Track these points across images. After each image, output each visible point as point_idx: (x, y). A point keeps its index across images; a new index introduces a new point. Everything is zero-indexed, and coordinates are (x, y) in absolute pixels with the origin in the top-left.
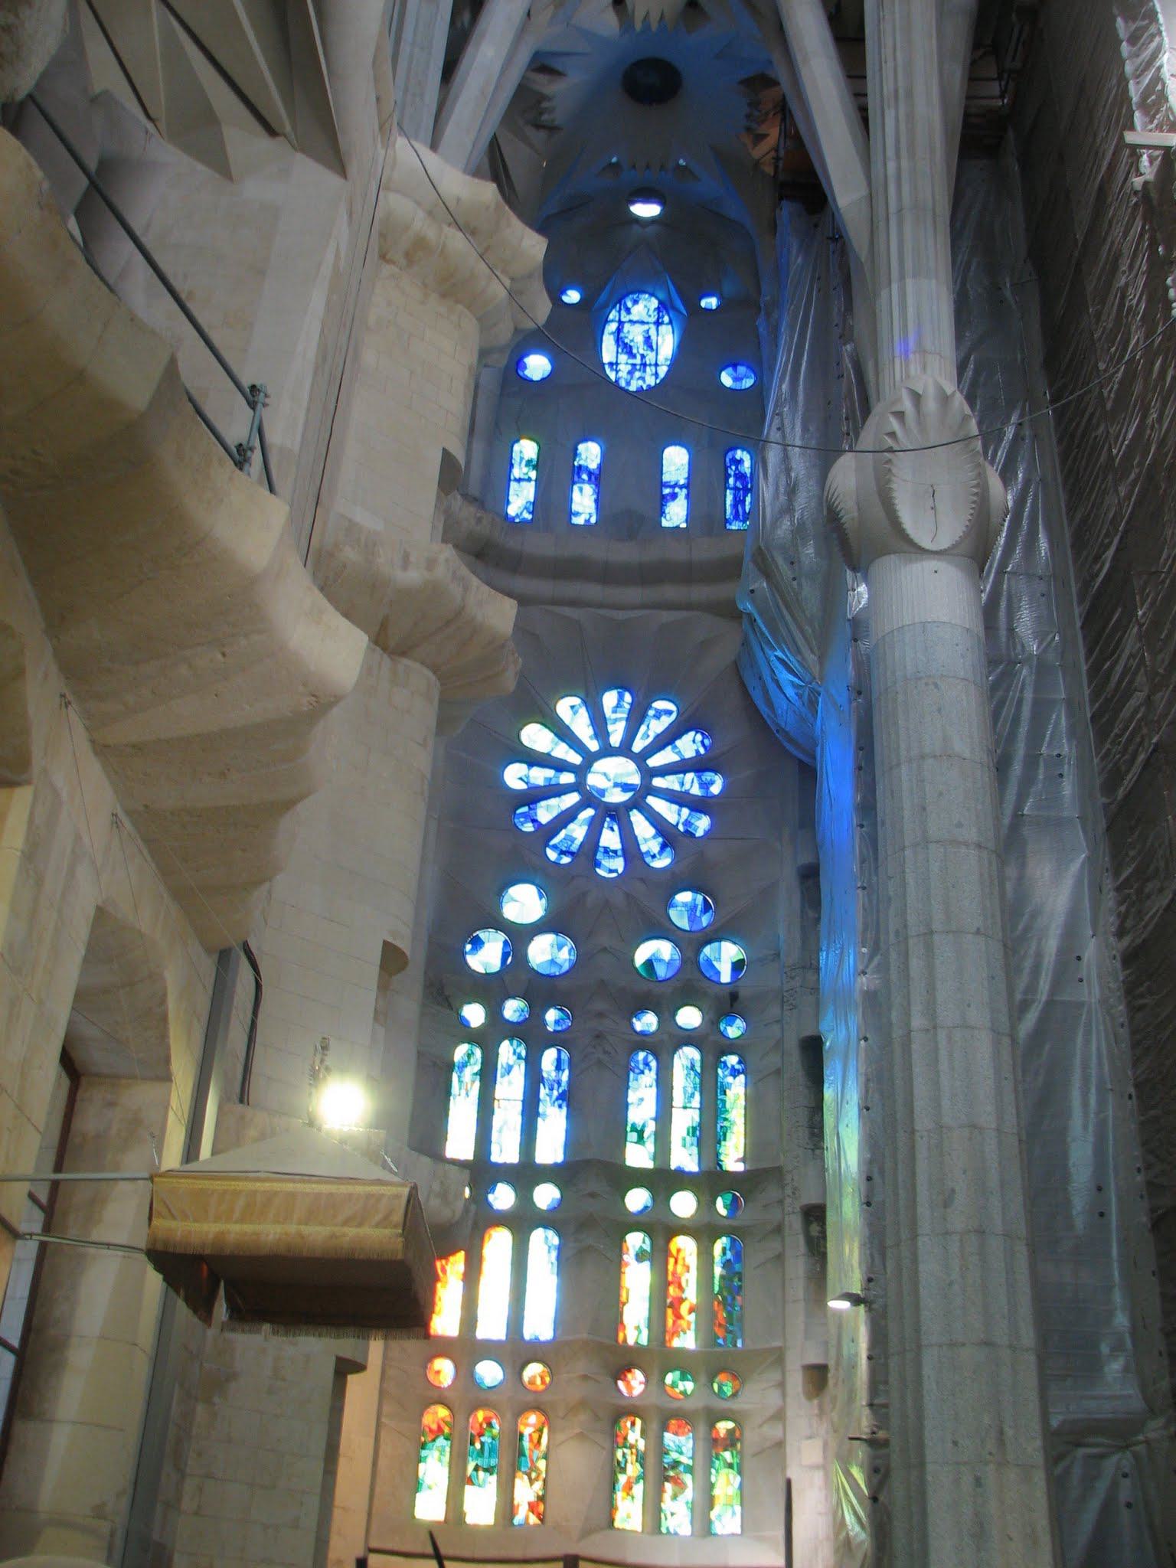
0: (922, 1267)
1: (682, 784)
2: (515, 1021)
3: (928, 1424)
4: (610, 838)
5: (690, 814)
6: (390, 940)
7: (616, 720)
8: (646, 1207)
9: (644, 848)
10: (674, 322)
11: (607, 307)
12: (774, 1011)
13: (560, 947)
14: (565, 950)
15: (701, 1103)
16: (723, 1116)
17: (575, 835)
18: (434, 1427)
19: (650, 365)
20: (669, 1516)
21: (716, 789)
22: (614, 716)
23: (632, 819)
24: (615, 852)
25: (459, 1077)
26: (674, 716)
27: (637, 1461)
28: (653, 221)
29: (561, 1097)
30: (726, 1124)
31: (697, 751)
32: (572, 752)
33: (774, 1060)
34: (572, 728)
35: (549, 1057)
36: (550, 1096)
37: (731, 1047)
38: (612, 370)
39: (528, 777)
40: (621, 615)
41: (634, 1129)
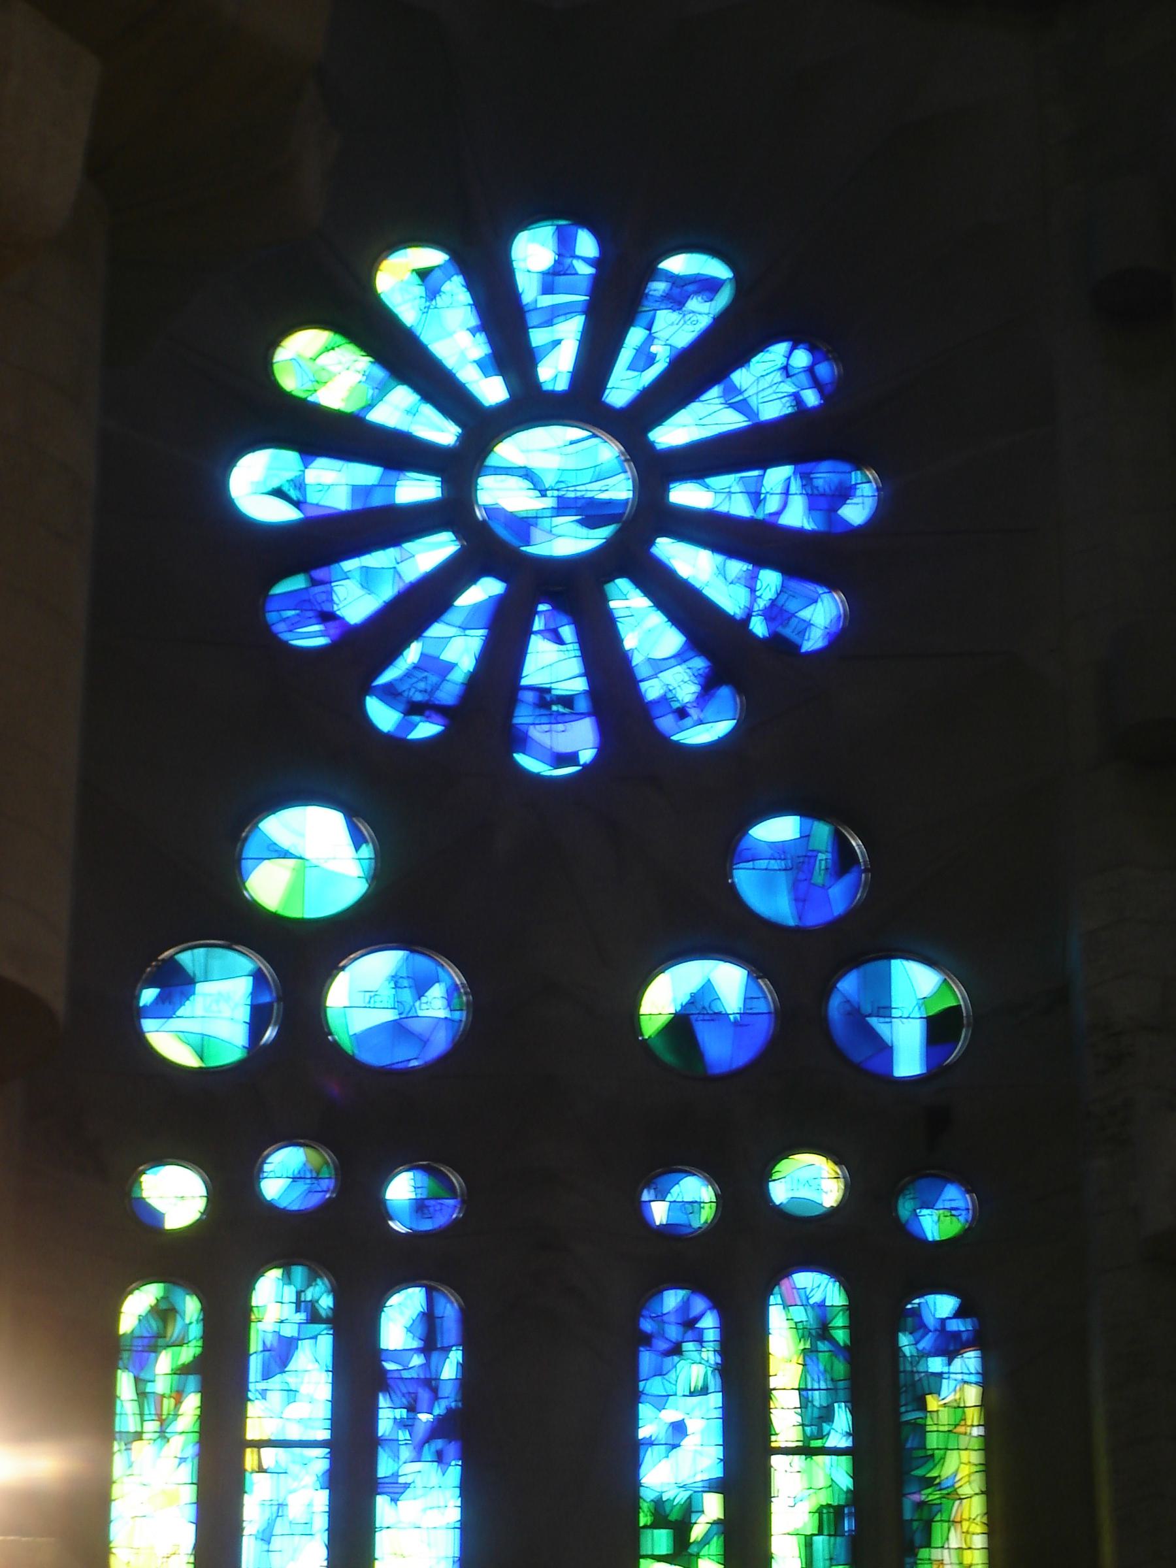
1: (756, 498)
2: (295, 1207)
5: (783, 589)
7: (552, 316)
9: (652, 690)
13: (421, 988)
14: (437, 992)
16: (919, 1472)
17: (447, 656)
21: (856, 512)
22: (547, 301)
24: (567, 701)
25: (137, 1380)
26: (724, 298)
29: (439, 1429)
30: (930, 1495)
31: (797, 398)
32: (428, 410)
34: (426, 337)
39: (300, 485)
41: (660, 1519)
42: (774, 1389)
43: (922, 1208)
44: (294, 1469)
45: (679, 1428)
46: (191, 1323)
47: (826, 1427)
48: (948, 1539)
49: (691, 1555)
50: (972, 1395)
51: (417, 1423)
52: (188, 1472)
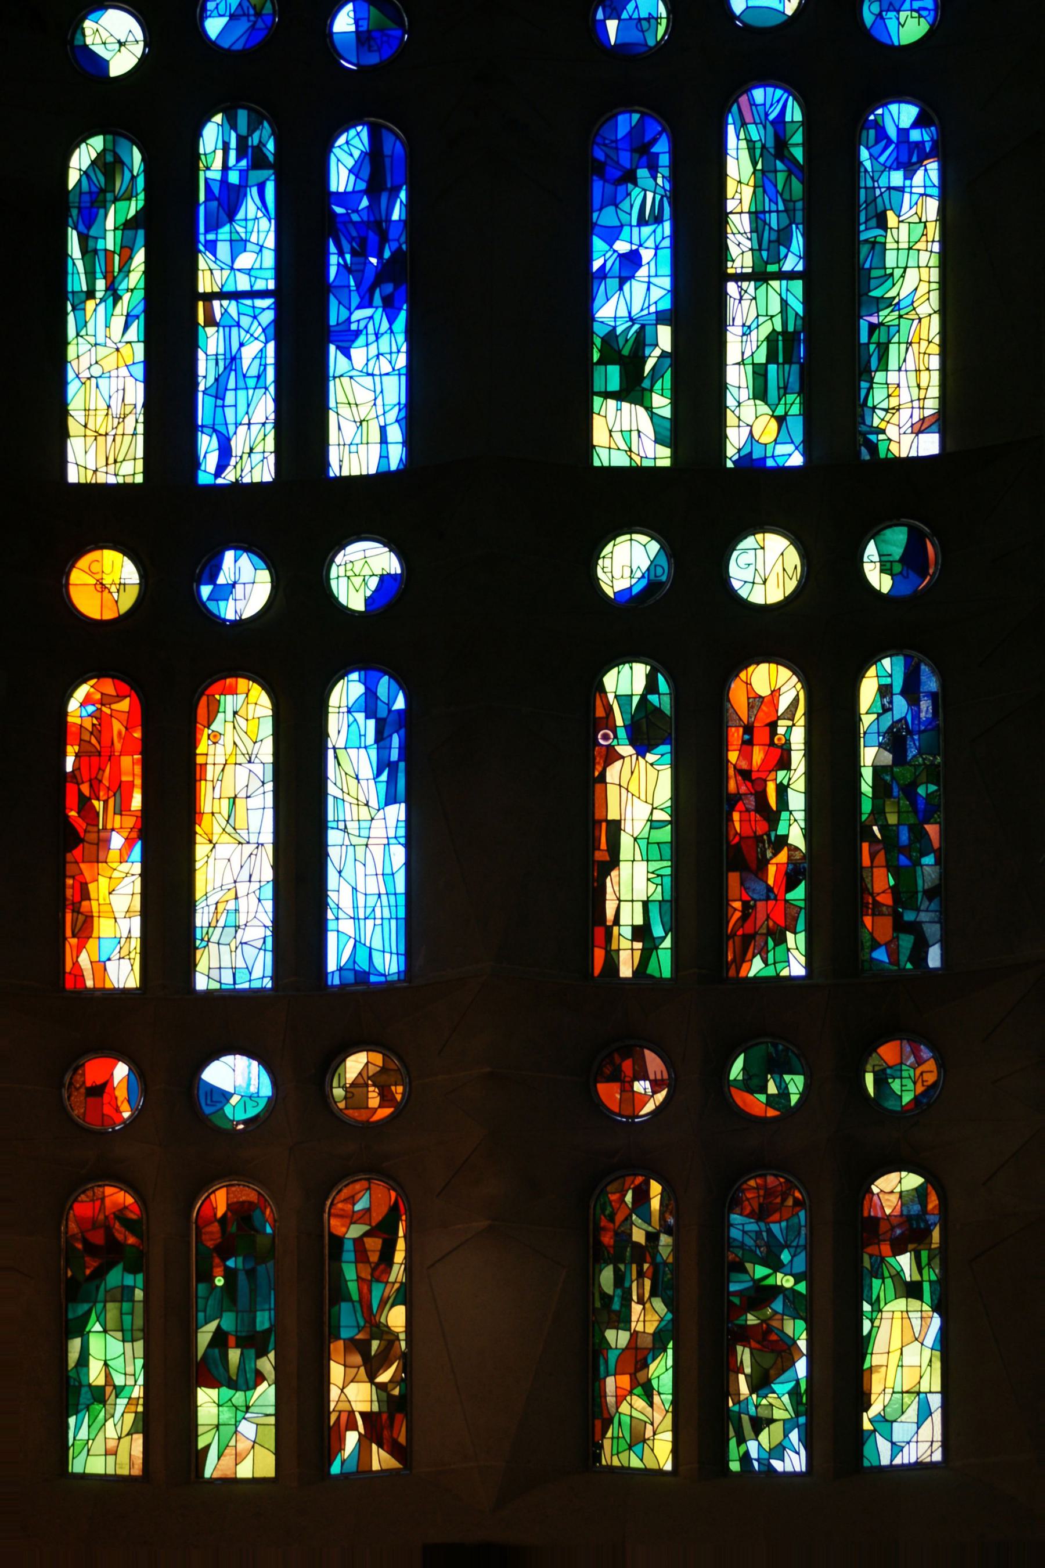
15: (808, 256)
30: (886, 316)
41: (611, 352)
42: (731, 213)
43: (888, 10)
44: (245, 321)
45: (631, 261)
46: (138, 175)
47: (783, 251)
48: (905, 360)
49: (644, 389)
50: (932, 207)
51: (368, 267)
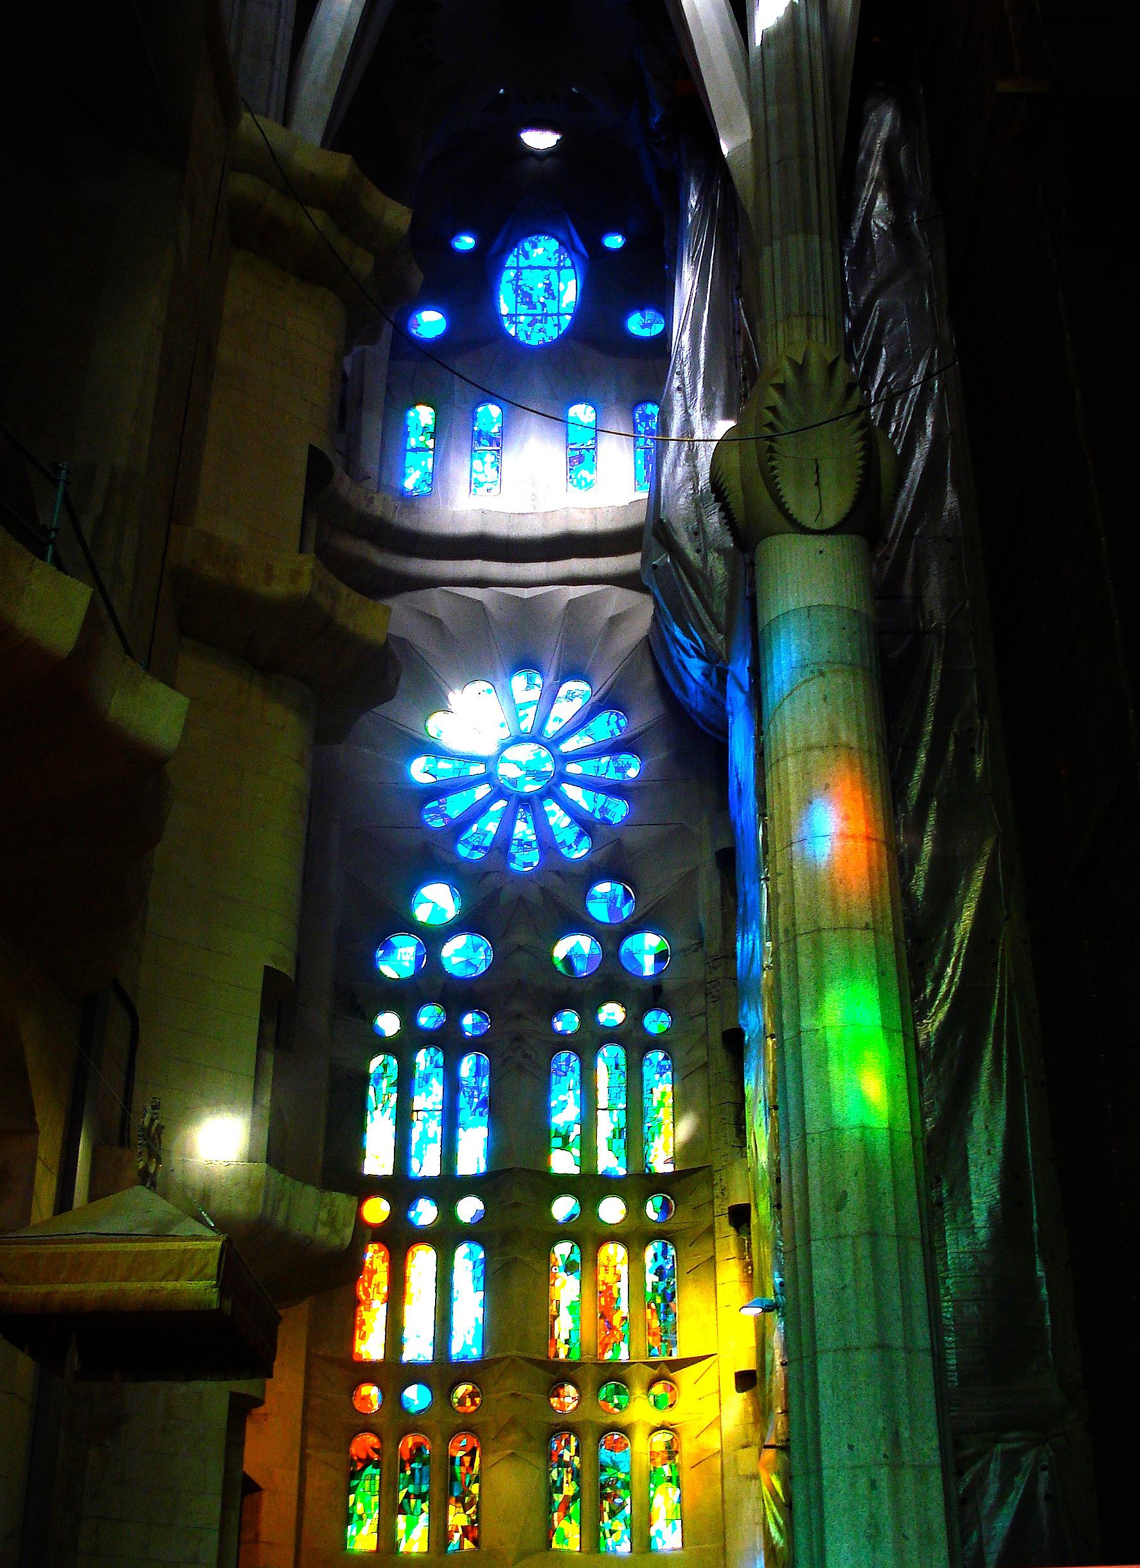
0: (816, 1272)
3: (824, 1430)
4: (523, 830)
6: (272, 965)
8: (573, 1216)
9: (559, 840)
10: (577, 267)
11: (506, 250)
12: (699, 1002)
13: (476, 948)
18: (363, 1456)
19: (552, 315)
20: (607, 1532)
21: (633, 773)
23: (547, 809)
24: (529, 844)
27: (572, 1480)
28: (550, 153)
29: (482, 1104)
33: (700, 1054)
35: (467, 1066)
36: (471, 1104)
37: (655, 1043)
38: (512, 322)
40: (526, 593)
52: (393, 1121)
